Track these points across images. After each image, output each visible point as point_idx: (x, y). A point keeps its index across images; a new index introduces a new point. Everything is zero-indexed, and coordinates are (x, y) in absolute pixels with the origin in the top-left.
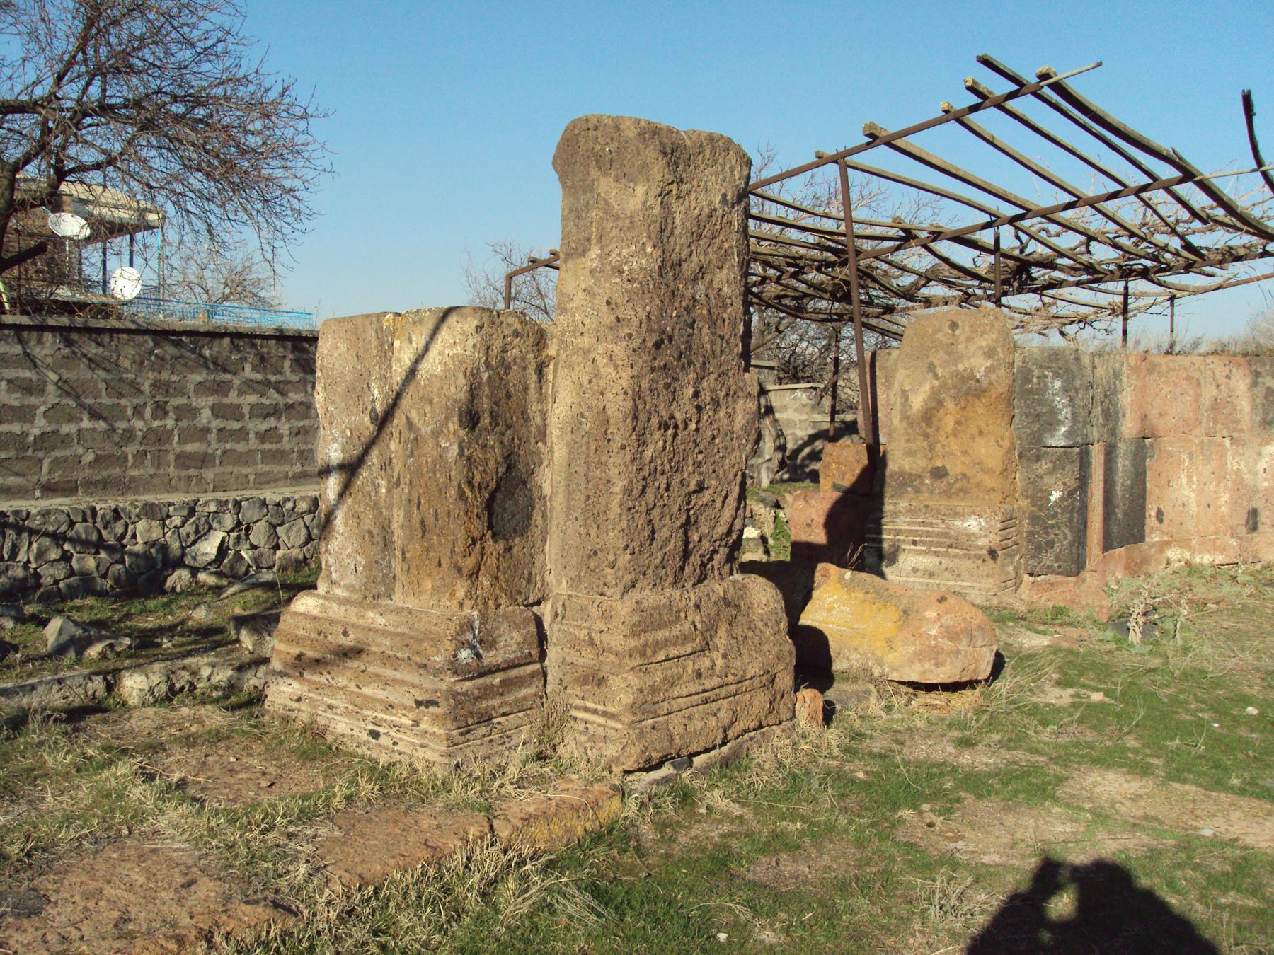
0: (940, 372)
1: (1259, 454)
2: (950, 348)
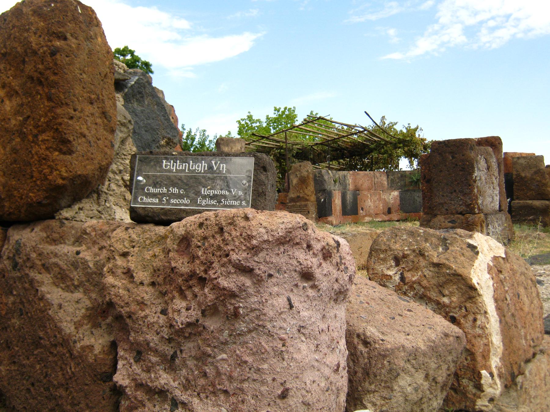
2: (299, 171)
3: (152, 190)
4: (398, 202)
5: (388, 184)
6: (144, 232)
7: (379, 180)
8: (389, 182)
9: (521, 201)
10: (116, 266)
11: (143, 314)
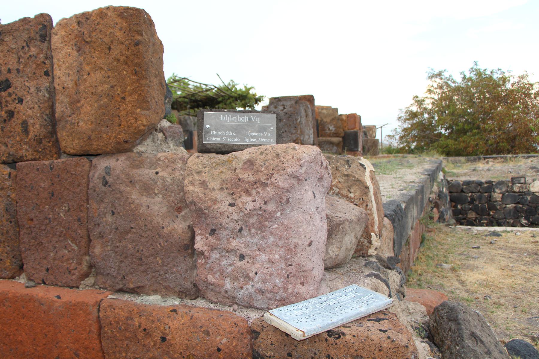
3: (215, 133)
6: (210, 158)
9: (324, 138)
10: (194, 180)
11: (216, 207)
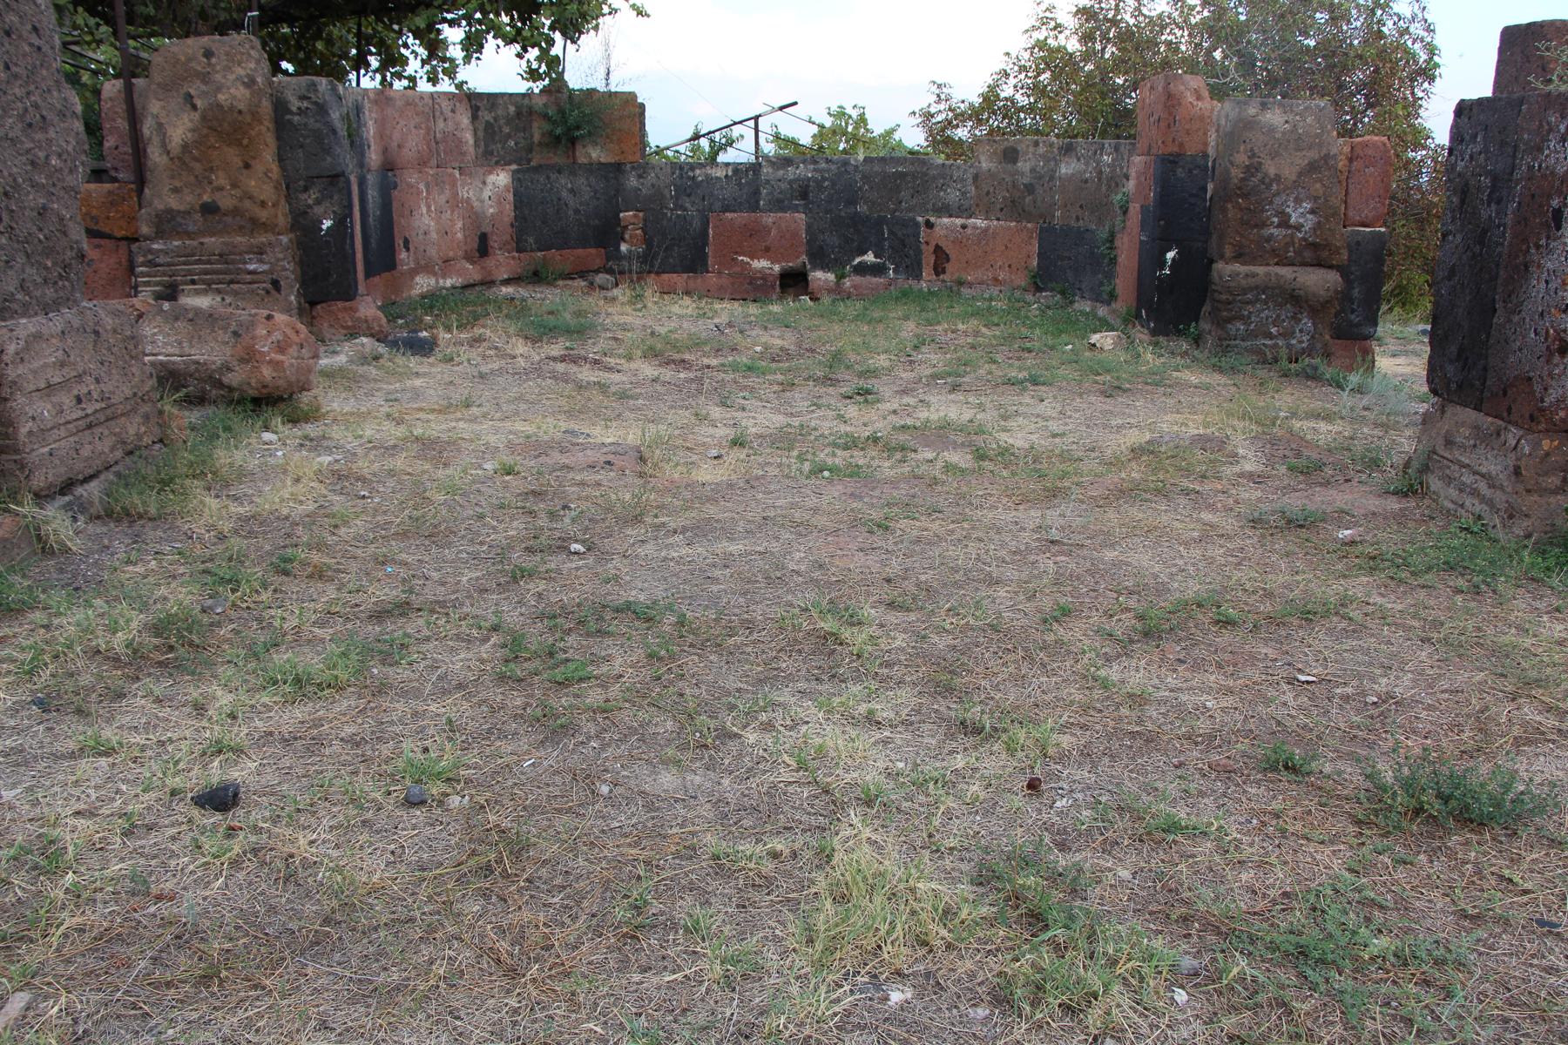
0: (199, 103)
1: (484, 183)
2: (205, 78)
4: (509, 208)
5: (476, 145)
7: (451, 126)
8: (481, 134)
9: (1260, 270)
